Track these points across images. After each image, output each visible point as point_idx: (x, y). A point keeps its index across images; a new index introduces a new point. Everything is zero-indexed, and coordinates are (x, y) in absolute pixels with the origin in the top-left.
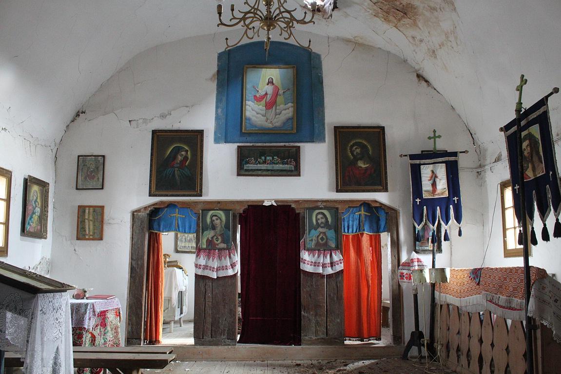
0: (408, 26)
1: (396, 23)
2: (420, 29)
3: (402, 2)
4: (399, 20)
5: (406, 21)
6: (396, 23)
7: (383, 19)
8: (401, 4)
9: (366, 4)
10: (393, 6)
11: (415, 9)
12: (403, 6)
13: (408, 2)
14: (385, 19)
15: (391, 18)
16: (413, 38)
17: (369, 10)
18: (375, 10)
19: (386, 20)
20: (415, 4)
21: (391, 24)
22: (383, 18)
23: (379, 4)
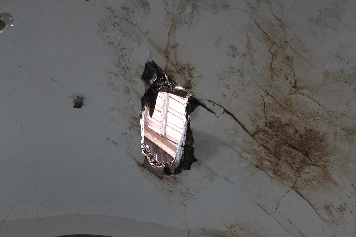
0: (314, 182)
1: (294, 179)
2: (335, 183)
3: (298, 128)
4: (299, 171)
5: (311, 171)
6: (294, 179)
7: (271, 173)
8: (297, 132)
9: (239, 140)
10: (284, 137)
11: (322, 141)
12: (301, 136)
13: (309, 127)
14: (275, 173)
15: (285, 168)
16: (327, 208)
17: (245, 155)
18: (255, 152)
19: (278, 174)
20: (319, 129)
21: (286, 182)
22: (270, 169)
23: (260, 135)
